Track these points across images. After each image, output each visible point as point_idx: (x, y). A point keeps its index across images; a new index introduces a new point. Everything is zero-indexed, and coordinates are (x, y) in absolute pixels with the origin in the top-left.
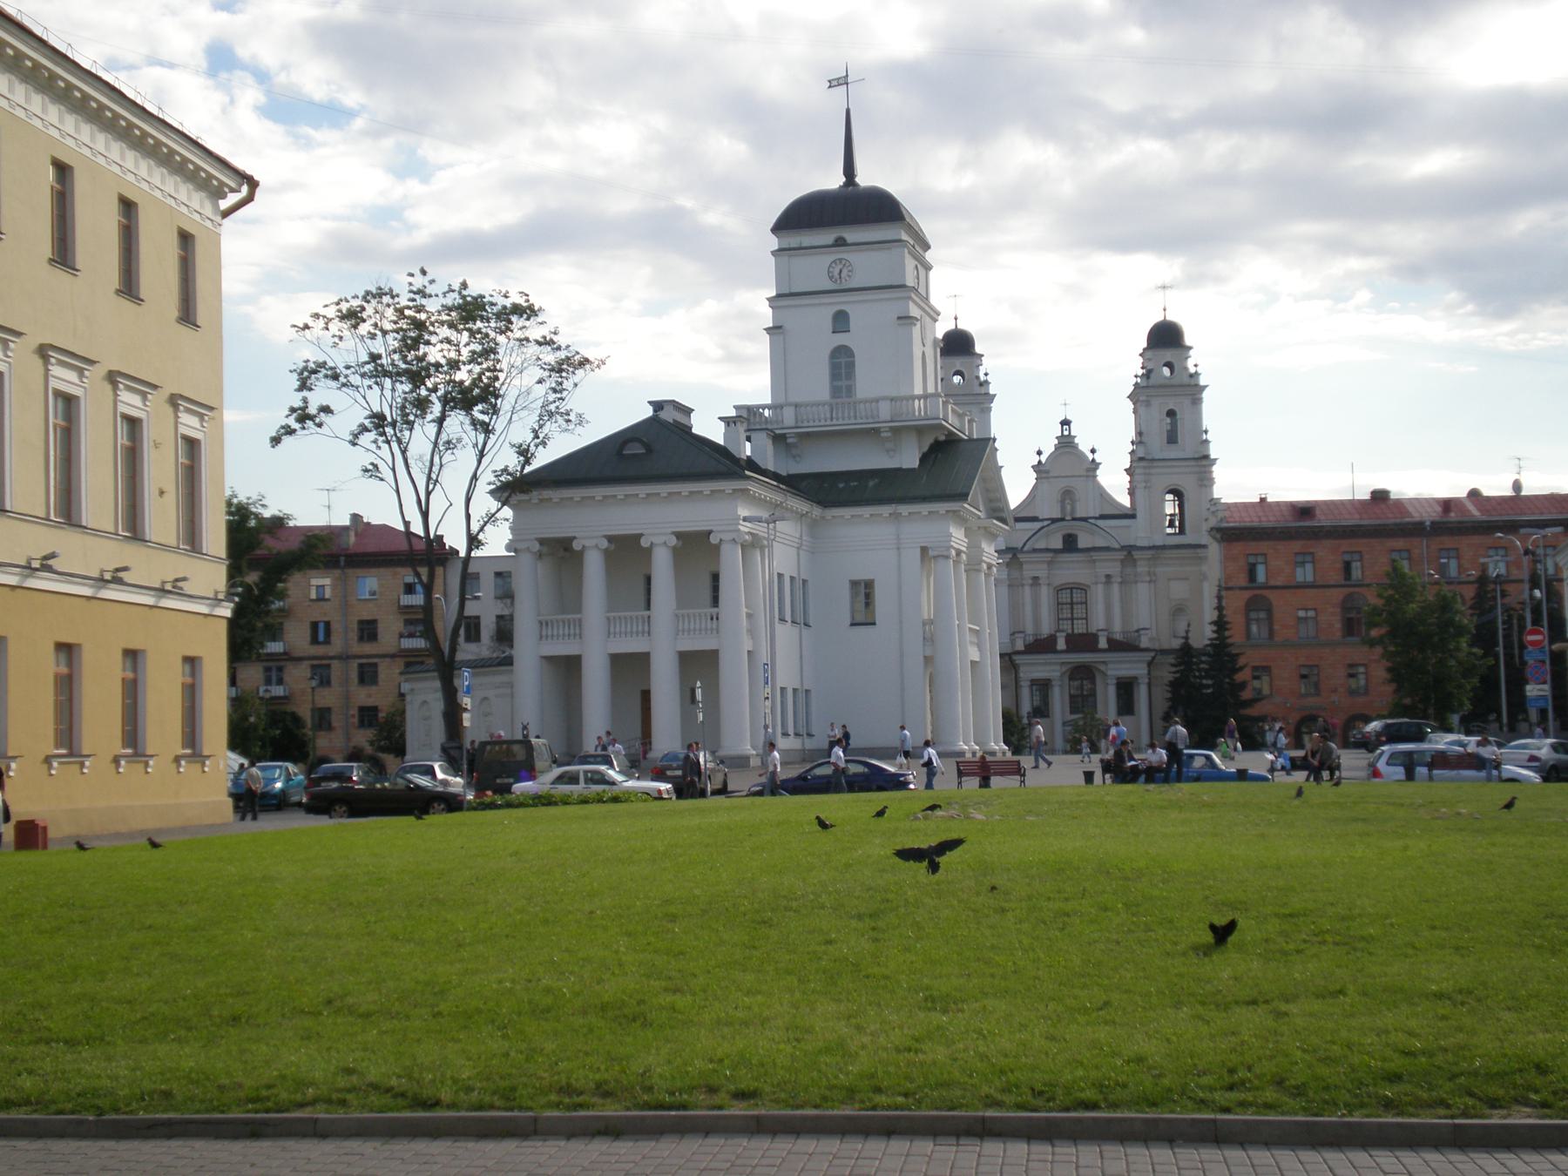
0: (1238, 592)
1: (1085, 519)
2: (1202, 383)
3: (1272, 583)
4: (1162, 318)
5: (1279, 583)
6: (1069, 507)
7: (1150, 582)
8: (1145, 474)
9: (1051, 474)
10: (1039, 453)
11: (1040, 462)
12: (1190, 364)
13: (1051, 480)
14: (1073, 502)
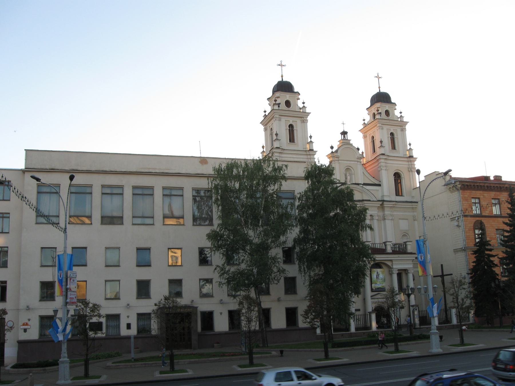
0: (469, 218)
1: (358, 184)
2: (405, 120)
3: (484, 214)
4: (378, 91)
5: (487, 215)
6: (349, 178)
7: (392, 220)
8: (385, 163)
9: (340, 159)
10: (332, 148)
11: (332, 152)
12: (397, 113)
13: (340, 162)
14: (351, 175)
